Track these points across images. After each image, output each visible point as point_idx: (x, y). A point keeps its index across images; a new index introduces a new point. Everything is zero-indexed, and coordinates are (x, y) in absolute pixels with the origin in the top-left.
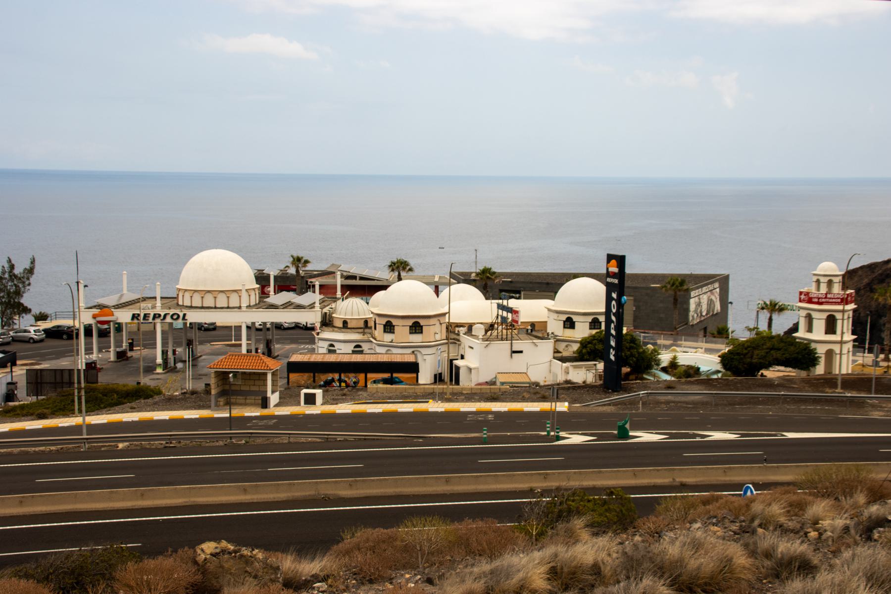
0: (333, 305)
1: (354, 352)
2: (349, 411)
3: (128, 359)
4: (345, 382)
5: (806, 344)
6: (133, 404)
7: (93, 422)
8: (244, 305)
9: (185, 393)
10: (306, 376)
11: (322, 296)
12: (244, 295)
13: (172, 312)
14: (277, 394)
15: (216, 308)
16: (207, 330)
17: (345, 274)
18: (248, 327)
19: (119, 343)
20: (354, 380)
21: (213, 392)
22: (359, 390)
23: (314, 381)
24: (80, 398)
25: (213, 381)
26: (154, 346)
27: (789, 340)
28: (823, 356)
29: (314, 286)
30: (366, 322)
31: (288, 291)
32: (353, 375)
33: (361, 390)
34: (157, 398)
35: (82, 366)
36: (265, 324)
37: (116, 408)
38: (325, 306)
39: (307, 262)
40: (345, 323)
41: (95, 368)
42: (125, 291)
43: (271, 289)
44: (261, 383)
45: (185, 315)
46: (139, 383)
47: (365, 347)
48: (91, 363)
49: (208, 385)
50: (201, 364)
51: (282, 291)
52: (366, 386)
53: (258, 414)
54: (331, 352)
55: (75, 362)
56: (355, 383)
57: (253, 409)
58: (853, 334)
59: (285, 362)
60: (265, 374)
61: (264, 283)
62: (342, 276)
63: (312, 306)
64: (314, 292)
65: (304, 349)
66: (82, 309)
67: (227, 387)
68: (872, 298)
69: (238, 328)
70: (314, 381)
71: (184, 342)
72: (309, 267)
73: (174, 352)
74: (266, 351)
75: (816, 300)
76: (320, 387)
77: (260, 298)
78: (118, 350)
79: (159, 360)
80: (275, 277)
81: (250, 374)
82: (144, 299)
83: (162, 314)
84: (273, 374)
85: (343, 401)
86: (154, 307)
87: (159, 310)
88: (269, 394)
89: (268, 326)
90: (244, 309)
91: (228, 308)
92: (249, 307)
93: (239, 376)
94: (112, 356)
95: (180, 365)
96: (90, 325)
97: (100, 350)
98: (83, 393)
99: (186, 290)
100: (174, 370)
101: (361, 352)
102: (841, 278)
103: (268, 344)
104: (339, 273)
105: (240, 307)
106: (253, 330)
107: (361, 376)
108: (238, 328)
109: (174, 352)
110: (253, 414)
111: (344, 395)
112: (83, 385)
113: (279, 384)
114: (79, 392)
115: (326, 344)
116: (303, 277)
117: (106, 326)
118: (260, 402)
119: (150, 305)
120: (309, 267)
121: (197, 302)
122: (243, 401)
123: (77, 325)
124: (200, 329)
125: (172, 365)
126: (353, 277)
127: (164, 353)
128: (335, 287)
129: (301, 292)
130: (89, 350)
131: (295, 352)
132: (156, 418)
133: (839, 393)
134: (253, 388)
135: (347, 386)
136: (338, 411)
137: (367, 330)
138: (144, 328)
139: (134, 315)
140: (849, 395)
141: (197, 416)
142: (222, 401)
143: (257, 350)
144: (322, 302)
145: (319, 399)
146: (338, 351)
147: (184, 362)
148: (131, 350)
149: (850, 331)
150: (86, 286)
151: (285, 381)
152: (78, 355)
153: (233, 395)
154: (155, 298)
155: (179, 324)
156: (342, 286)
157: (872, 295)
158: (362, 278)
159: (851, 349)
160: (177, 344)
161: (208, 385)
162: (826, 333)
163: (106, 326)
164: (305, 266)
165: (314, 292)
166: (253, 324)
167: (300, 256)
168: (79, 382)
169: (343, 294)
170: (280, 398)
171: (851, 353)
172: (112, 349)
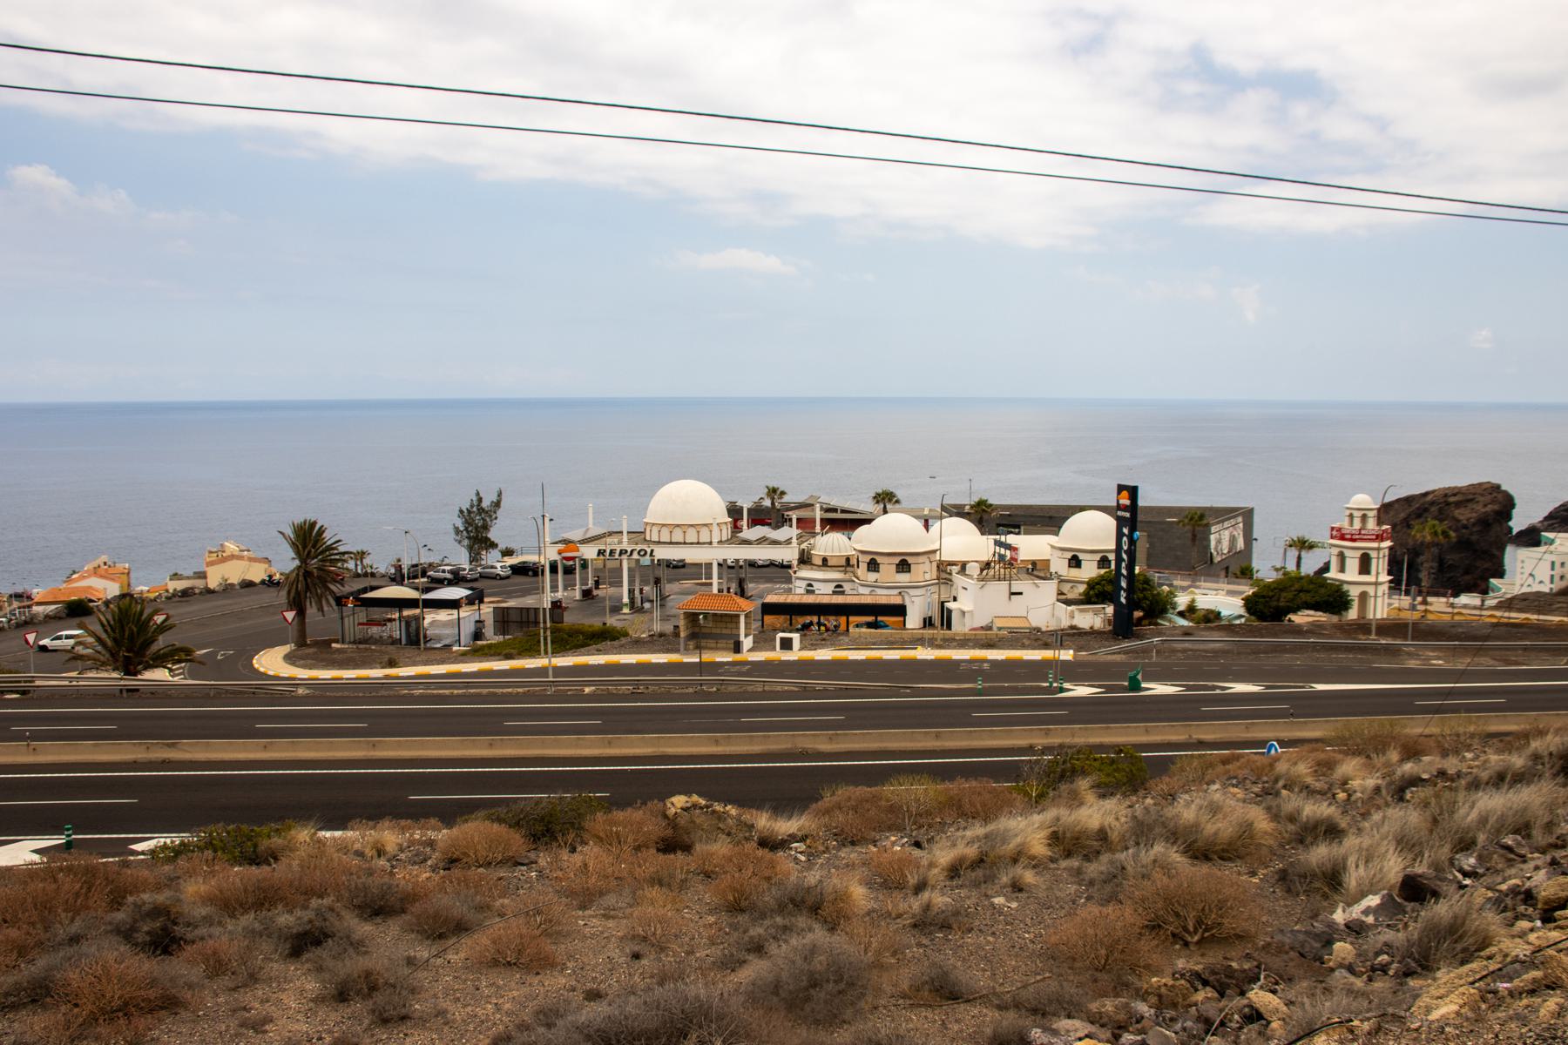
0: (812, 541)
1: (834, 593)
2: (830, 658)
3: (593, 597)
4: (825, 625)
5: (1338, 586)
6: (599, 646)
7: (559, 665)
8: (715, 540)
9: (652, 635)
10: (782, 618)
11: (799, 531)
12: (715, 529)
13: (639, 548)
14: (750, 638)
15: (685, 543)
16: (675, 567)
17: (825, 506)
18: (719, 565)
19: (584, 581)
20: (835, 623)
21: (682, 635)
22: (839, 634)
23: (791, 624)
24: (545, 639)
25: (682, 623)
26: (620, 584)
27: (1320, 580)
28: (1356, 599)
29: (791, 520)
30: (848, 560)
31: (763, 525)
32: (834, 618)
33: (842, 634)
34: (623, 640)
35: (547, 605)
36: (737, 561)
37: (582, 650)
38: (803, 542)
39: (783, 493)
40: (825, 560)
41: (560, 607)
42: (591, 526)
43: (744, 523)
44: (733, 625)
45: (652, 551)
46: (605, 624)
47: (847, 587)
48: (556, 602)
49: (676, 627)
50: (669, 604)
51: (756, 525)
52: (848, 630)
53: (730, 659)
54: (808, 592)
55: (541, 600)
56: (835, 626)
57: (725, 653)
58: (1389, 574)
59: (759, 602)
60: (738, 616)
61: (736, 516)
62: (822, 508)
63: (788, 542)
64: (791, 526)
65: (779, 589)
66: (547, 544)
67: (697, 630)
68: (1409, 534)
69: (709, 565)
70: (791, 624)
71: (652, 581)
72: (786, 499)
73: (641, 590)
74: (739, 591)
75: (1348, 537)
76: (797, 630)
77: (732, 532)
78: (584, 588)
79: (626, 600)
80: (749, 510)
81: (722, 615)
82: (611, 534)
83: (629, 550)
84: (746, 616)
85: (823, 647)
86: (620, 542)
87: (625, 546)
88: (742, 638)
89: (741, 563)
90: (715, 544)
91: (698, 543)
92: (720, 542)
93: (710, 618)
94: (578, 595)
95: (647, 605)
96: (556, 561)
97: (565, 589)
98: (549, 633)
99: (654, 524)
100: (641, 610)
101: (842, 593)
102: (1375, 512)
103: (741, 583)
104: (818, 505)
105: (711, 543)
106: (725, 567)
107: (843, 619)
108: (709, 565)
109: (641, 590)
110: (725, 660)
111: (824, 640)
112: (548, 625)
113: (753, 627)
114: (545, 633)
115: (803, 584)
116: (779, 510)
117: (571, 563)
118: (732, 646)
119: (616, 540)
120: (786, 499)
121: (665, 538)
122: (713, 645)
123: (543, 562)
124: (668, 566)
125: (639, 605)
126: (834, 510)
127: (631, 592)
128: (814, 521)
129: (777, 527)
130: (554, 588)
131: (770, 592)
132: (622, 662)
134: (724, 631)
135: (827, 630)
136: (817, 658)
137: (848, 569)
138: (610, 564)
139: (600, 550)
140: (1384, 642)
141: (666, 661)
142: (691, 644)
143: (729, 589)
144: (799, 537)
145: (796, 644)
146: (817, 592)
147: (652, 601)
148: (597, 588)
149: (1386, 572)
150: (551, 520)
151: (760, 623)
152: (543, 593)
153: (703, 638)
154: (621, 532)
155: (646, 561)
156: (822, 520)
157: (1409, 531)
158: (843, 511)
159: (1387, 592)
160: (644, 582)
161: (676, 627)
162: (1360, 573)
163: (571, 563)
164: (781, 498)
165: (791, 526)
166: (725, 560)
167: (776, 486)
168: (545, 622)
169: (822, 529)
170: (754, 642)
171: (1386, 596)
172: (577, 587)
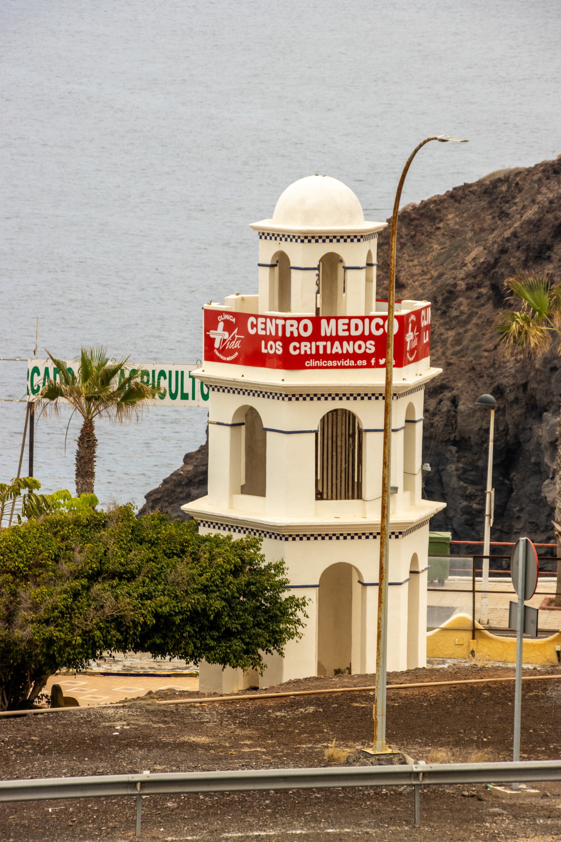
5: (240, 547)
27: (170, 529)
28: (312, 595)
58: (428, 494)
68: (504, 331)
75: (277, 348)
102: (372, 245)
133: (380, 759)
140: (422, 766)
149: (418, 483)
157: (500, 316)
159: (423, 562)
162: (319, 496)
171: (423, 578)
